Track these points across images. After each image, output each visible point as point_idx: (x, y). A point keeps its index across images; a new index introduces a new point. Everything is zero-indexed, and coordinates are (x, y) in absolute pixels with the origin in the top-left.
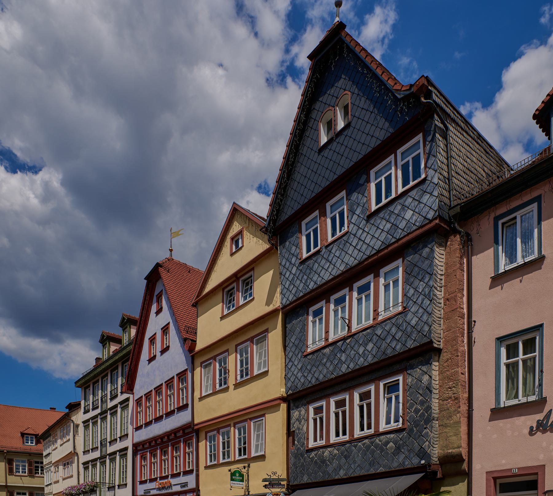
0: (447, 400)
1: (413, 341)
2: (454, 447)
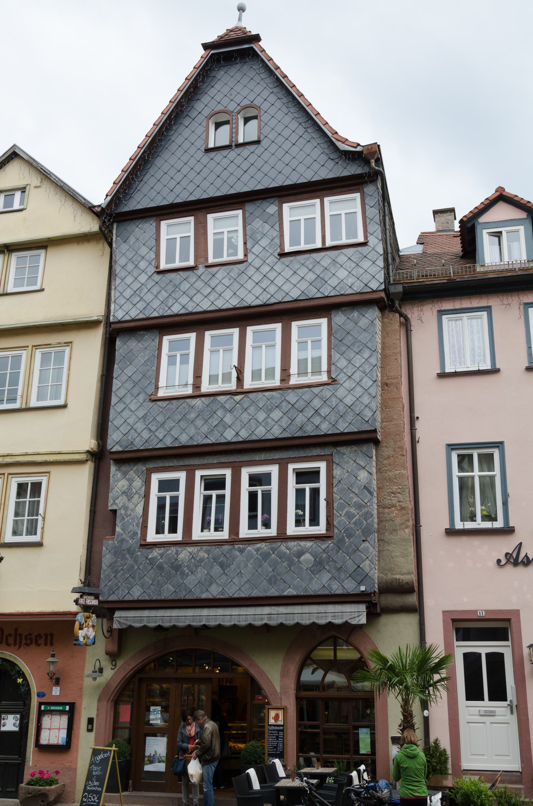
0: (389, 508)
1: (347, 424)
2: (402, 572)
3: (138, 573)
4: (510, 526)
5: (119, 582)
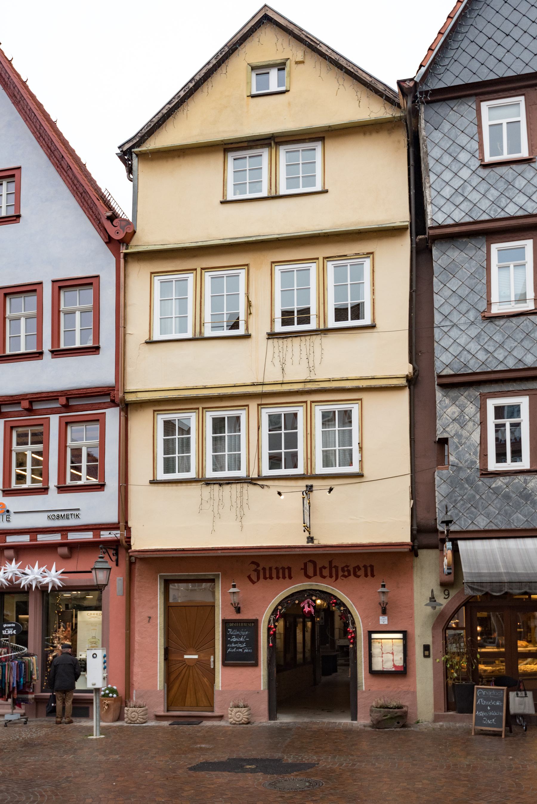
3: (480, 503)
5: (460, 512)
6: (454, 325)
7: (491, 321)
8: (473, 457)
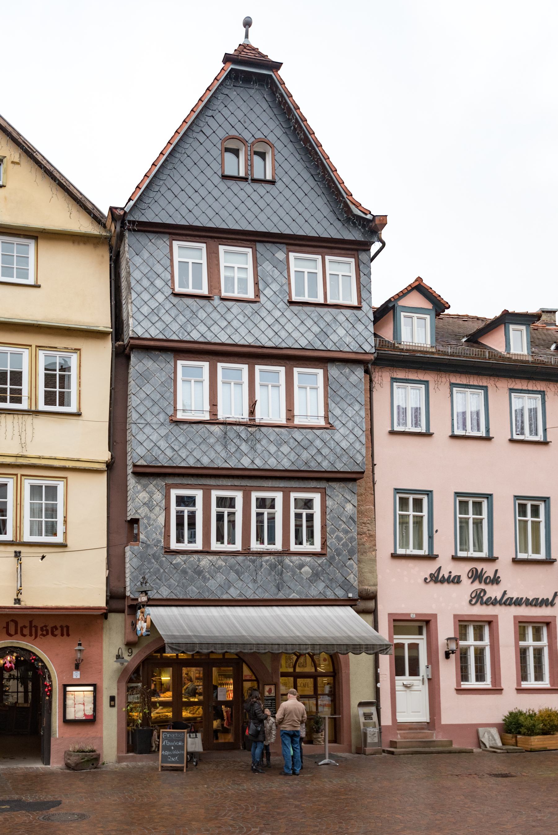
0: (361, 535)
4: (434, 554)
6: (148, 424)
7: (177, 425)
8: (159, 537)
